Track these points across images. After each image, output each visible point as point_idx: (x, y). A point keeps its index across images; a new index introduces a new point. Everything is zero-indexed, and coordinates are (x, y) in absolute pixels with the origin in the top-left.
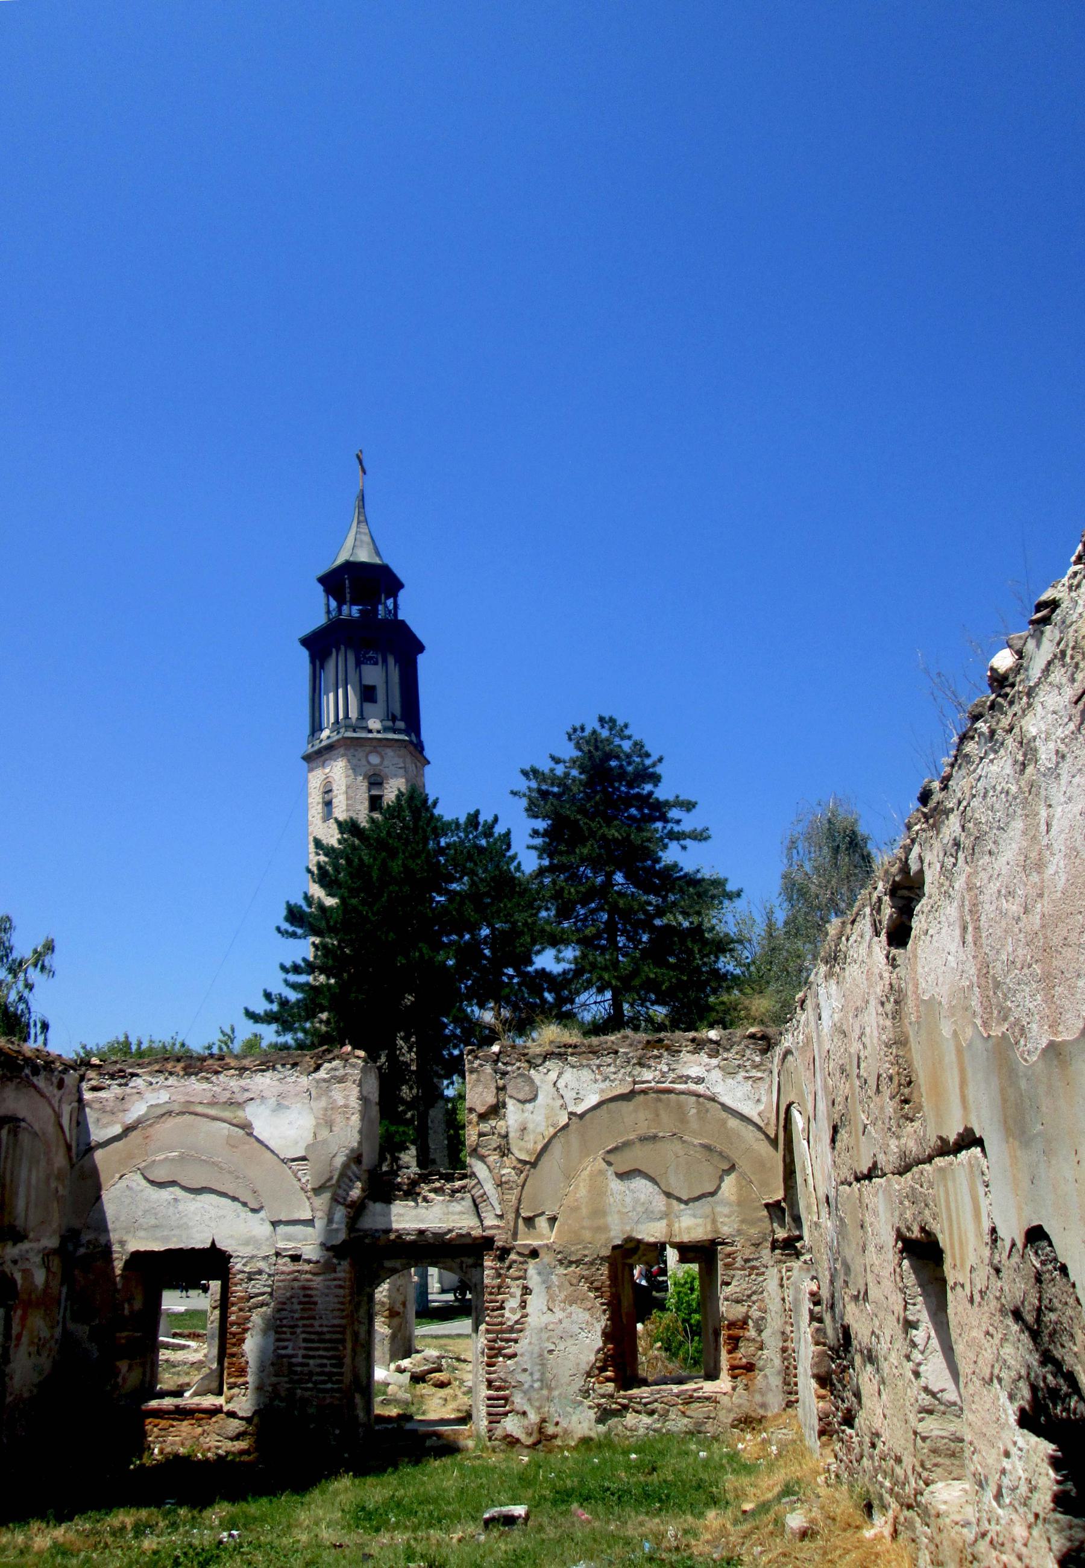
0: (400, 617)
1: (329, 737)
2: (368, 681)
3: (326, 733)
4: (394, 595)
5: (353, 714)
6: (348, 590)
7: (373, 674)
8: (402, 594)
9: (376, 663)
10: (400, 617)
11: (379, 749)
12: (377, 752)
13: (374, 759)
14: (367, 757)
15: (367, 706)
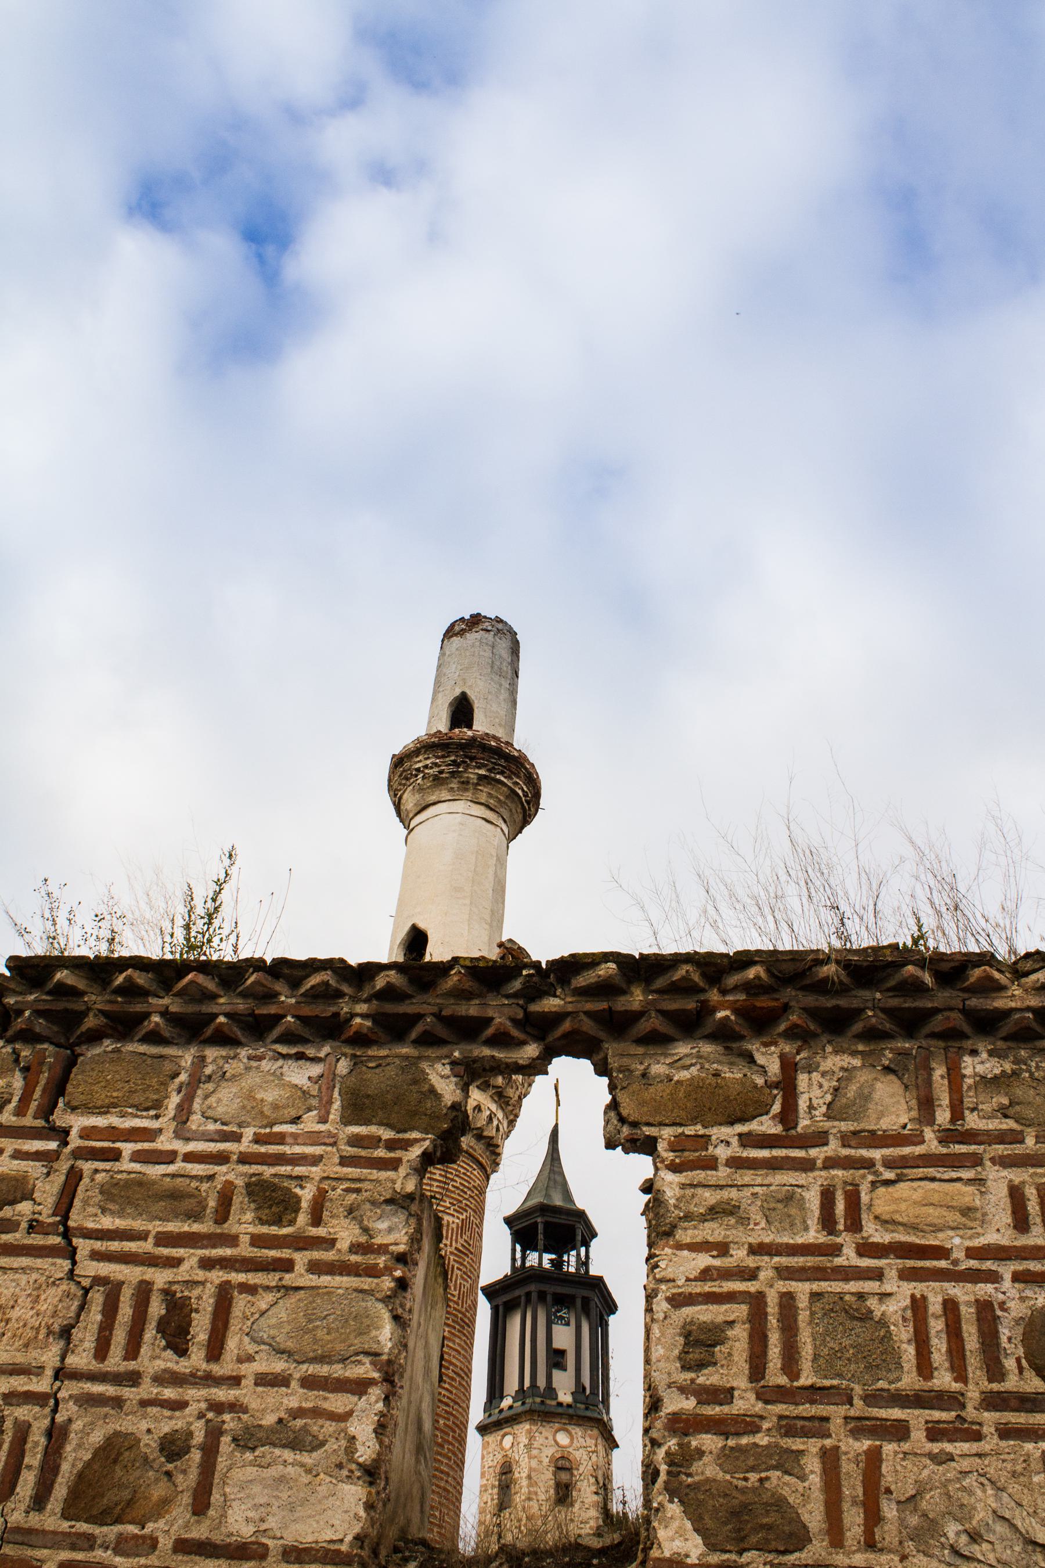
0: (593, 1272)
1: (511, 1407)
2: (557, 1344)
3: (507, 1402)
4: (586, 1244)
5: (542, 1383)
6: (540, 1236)
7: (563, 1337)
8: (594, 1243)
9: (568, 1324)
10: (593, 1272)
11: (569, 1427)
12: (567, 1431)
13: (563, 1439)
14: (556, 1432)
15: (557, 1374)
